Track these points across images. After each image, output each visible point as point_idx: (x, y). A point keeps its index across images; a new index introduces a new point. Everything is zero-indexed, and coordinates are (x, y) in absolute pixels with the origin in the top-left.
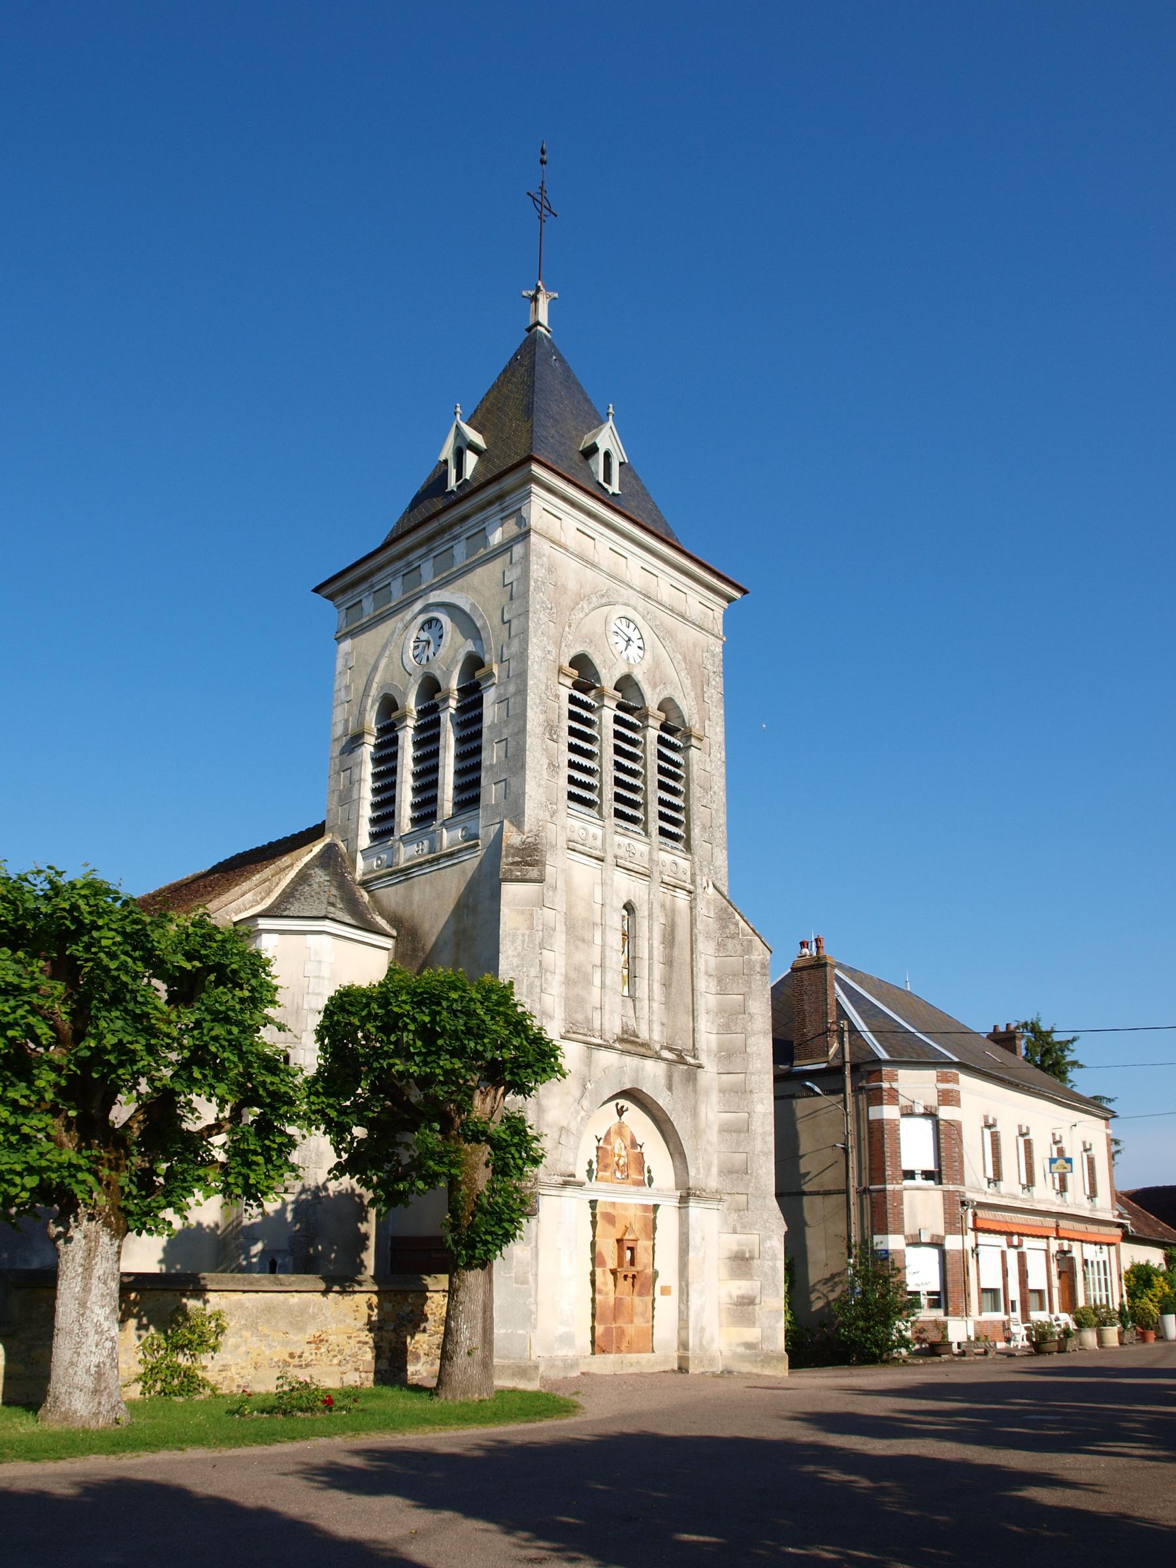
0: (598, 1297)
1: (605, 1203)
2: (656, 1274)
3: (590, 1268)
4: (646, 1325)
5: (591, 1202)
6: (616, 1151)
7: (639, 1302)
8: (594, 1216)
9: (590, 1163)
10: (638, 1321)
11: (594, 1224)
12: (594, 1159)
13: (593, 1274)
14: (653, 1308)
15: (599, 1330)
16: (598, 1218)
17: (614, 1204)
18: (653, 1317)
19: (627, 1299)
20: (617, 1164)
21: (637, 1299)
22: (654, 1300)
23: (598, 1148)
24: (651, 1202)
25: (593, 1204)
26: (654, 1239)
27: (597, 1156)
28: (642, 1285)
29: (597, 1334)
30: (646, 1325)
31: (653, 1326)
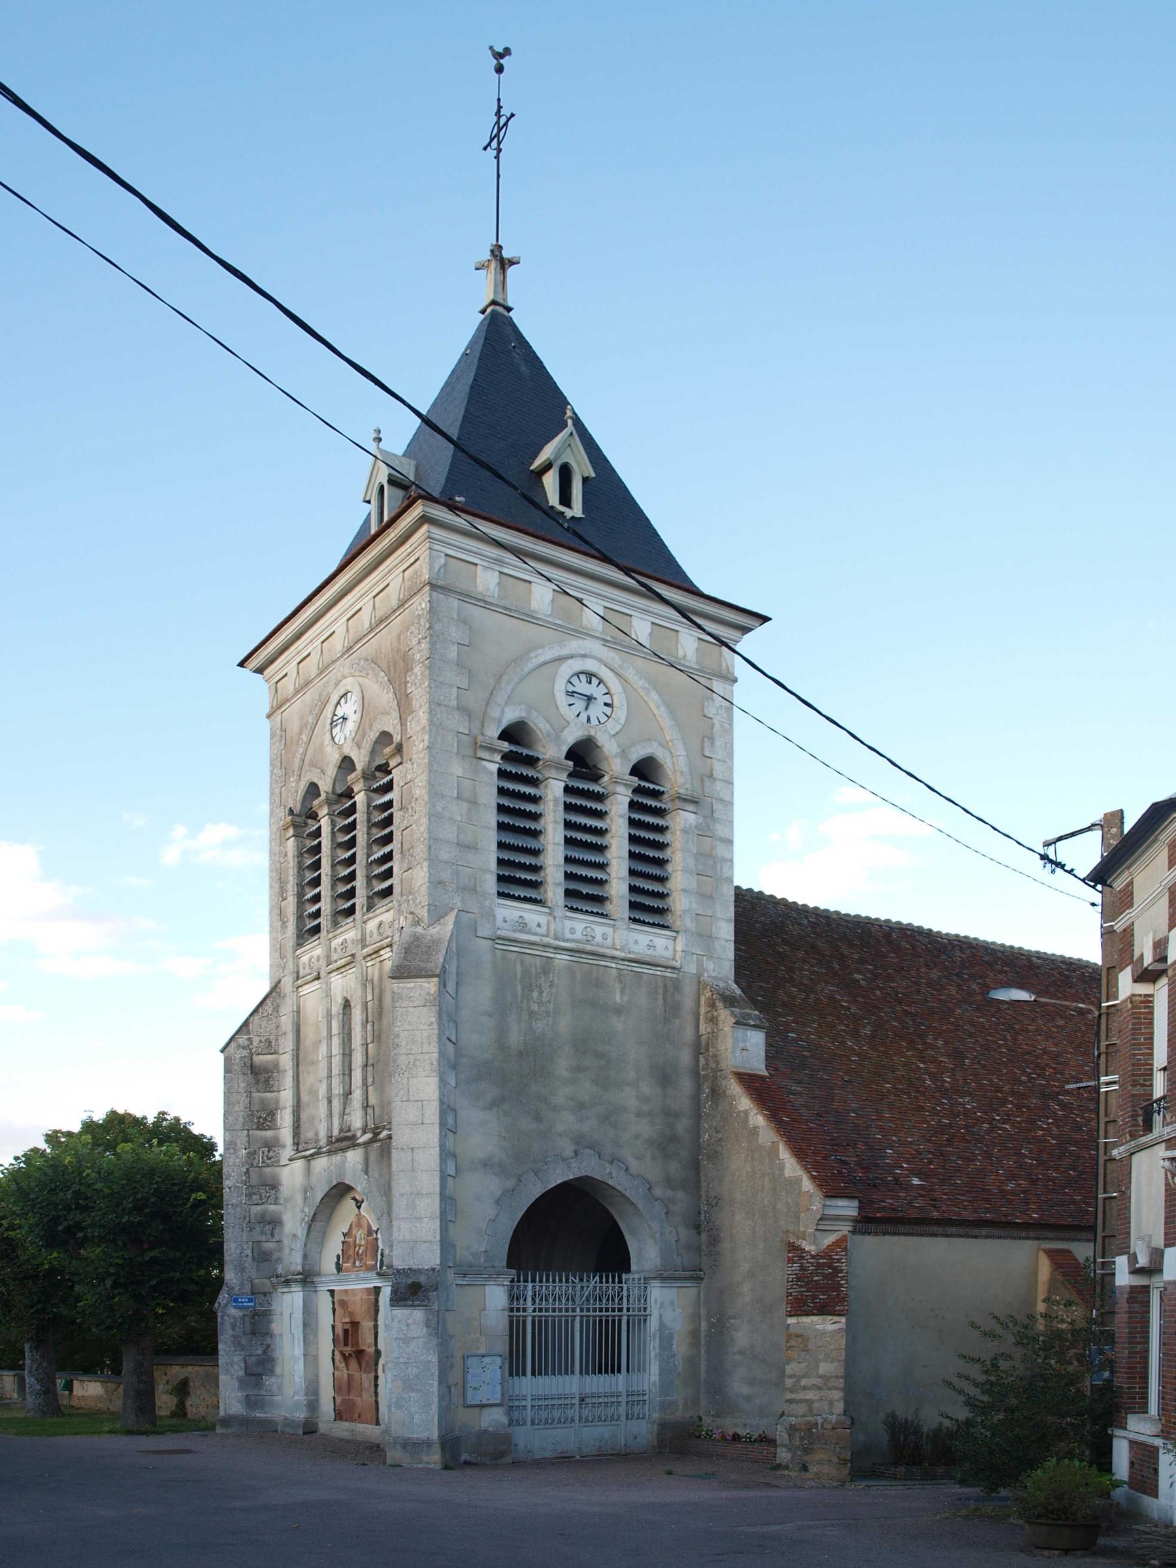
0: (336, 1373)
1: (340, 1291)
2: (378, 1353)
3: (333, 1348)
4: (370, 1399)
5: (328, 1290)
6: (357, 1242)
7: (366, 1379)
8: (333, 1303)
9: (338, 1257)
10: (365, 1395)
11: (334, 1310)
12: (341, 1254)
13: (333, 1351)
14: (376, 1386)
15: (338, 1400)
16: (336, 1306)
17: (346, 1290)
18: (376, 1394)
19: (357, 1375)
20: (358, 1254)
21: (364, 1375)
22: (376, 1378)
23: (343, 1243)
24: (371, 1286)
25: (332, 1292)
26: (376, 1320)
27: (343, 1250)
28: (367, 1364)
29: (337, 1404)
30: (370, 1399)
31: (377, 1402)
